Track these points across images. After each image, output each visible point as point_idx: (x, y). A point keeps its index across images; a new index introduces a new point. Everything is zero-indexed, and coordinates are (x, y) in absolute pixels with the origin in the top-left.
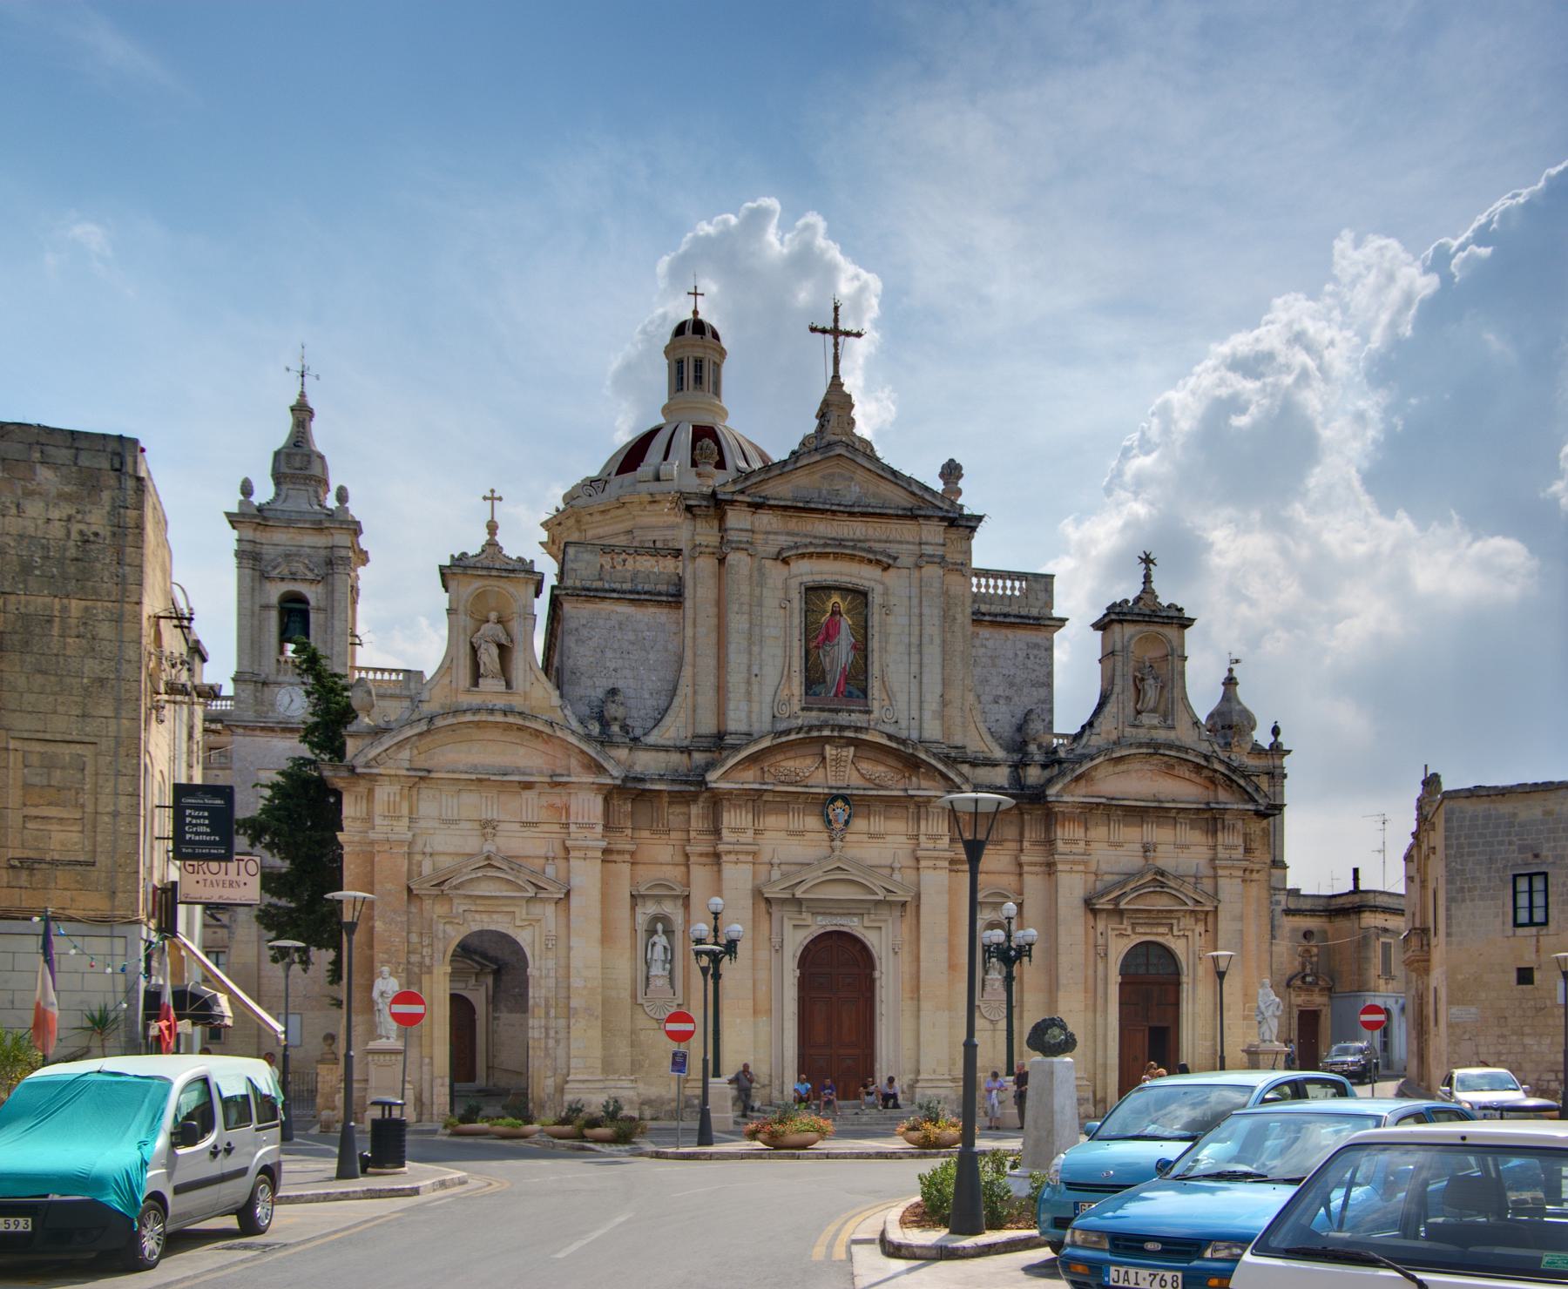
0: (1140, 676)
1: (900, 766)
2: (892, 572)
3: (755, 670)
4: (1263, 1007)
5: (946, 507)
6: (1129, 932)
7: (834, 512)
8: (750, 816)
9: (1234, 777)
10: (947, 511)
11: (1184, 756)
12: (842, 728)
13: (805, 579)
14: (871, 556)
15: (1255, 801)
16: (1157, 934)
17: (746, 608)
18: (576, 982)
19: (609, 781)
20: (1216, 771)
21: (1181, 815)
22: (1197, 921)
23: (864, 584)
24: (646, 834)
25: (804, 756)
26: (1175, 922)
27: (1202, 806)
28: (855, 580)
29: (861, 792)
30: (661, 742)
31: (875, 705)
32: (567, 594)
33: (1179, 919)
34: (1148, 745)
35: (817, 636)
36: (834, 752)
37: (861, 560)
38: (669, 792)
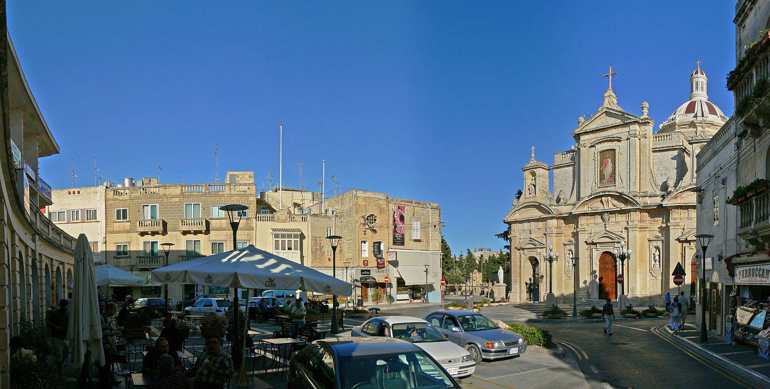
3: (587, 179)
12: (605, 192)
23: (614, 148)
31: (617, 183)
35: (603, 164)
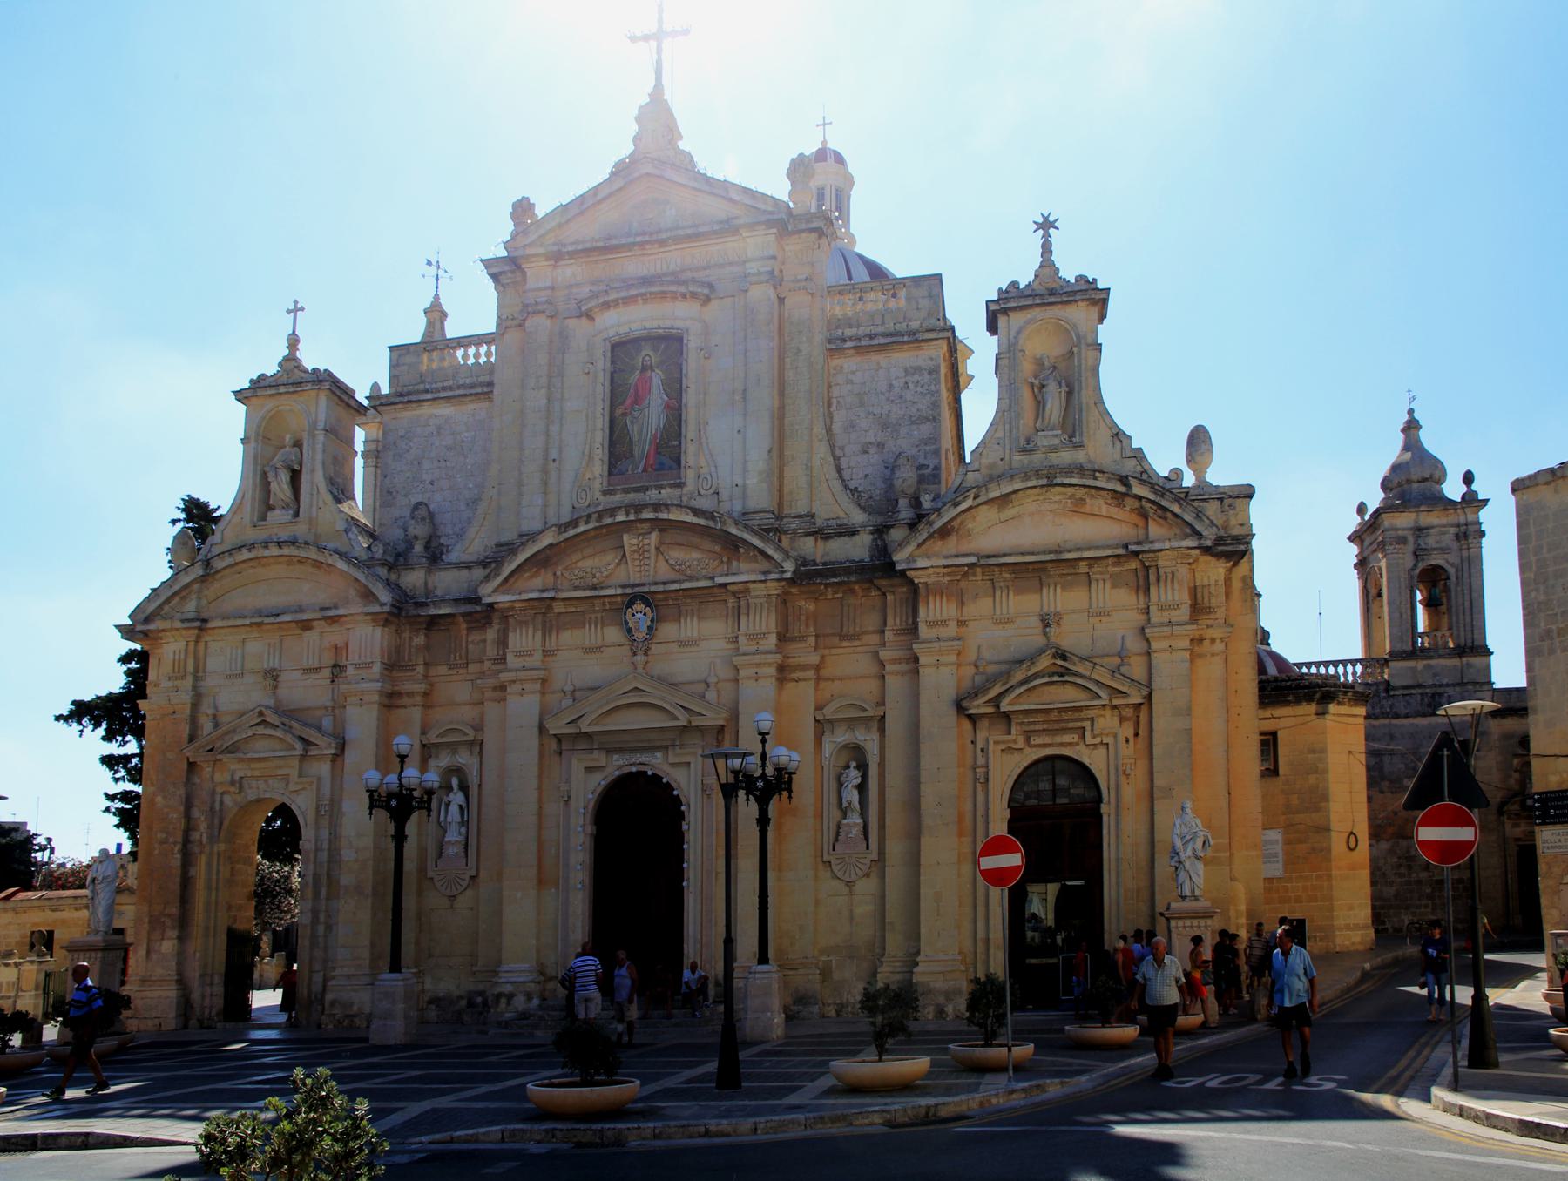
0: (1036, 382)
1: (718, 548)
2: (714, 304)
3: (554, 454)
4: (1179, 844)
5: (770, 209)
6: (1020, 744)
7: (642, 245)
8: (539, 634)
9: (1164, 503)
10: (771, 213)
11: (1091, 482)
13: (611, 333)
14: (682, 289)
15: (1196, 533)
16: (1062, 745)
17: (544, 381)
18: (347, 855)
19: (377, 609)
20: (1140, 498)
21: (1096, 569)
22: (1122, 719)
24: (443, 670)
25: (604, 551)
26: (1087, 724)
27: (1121, 551)
28: (668, 323)
29: (661, 588)
30: (465, 558)
31: (690, 476)
32: (382, 404)
33: (1092, 720)
34: (1037, 474)
36: (635, 541)
37: (674, 297)
38: (464, 615)
